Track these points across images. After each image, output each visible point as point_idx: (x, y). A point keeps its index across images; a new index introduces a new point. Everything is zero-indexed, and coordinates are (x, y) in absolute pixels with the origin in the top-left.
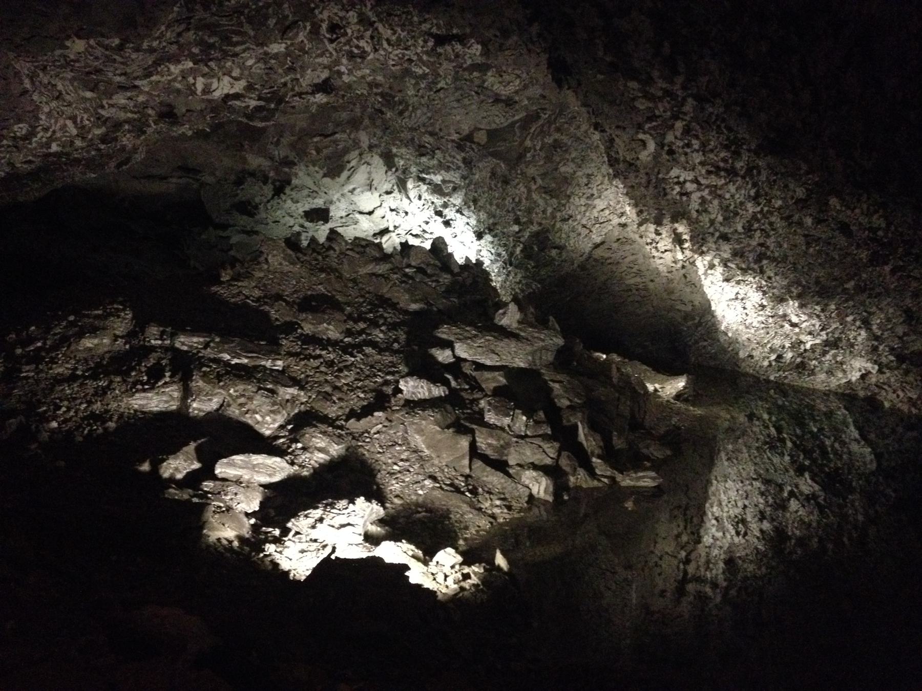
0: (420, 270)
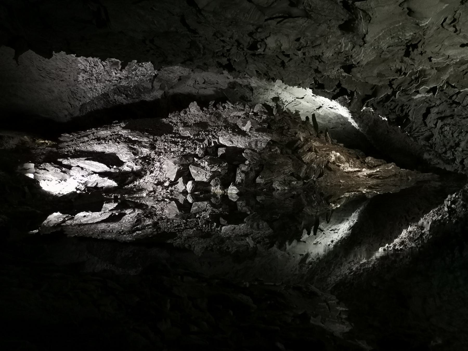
0: (256, 114)
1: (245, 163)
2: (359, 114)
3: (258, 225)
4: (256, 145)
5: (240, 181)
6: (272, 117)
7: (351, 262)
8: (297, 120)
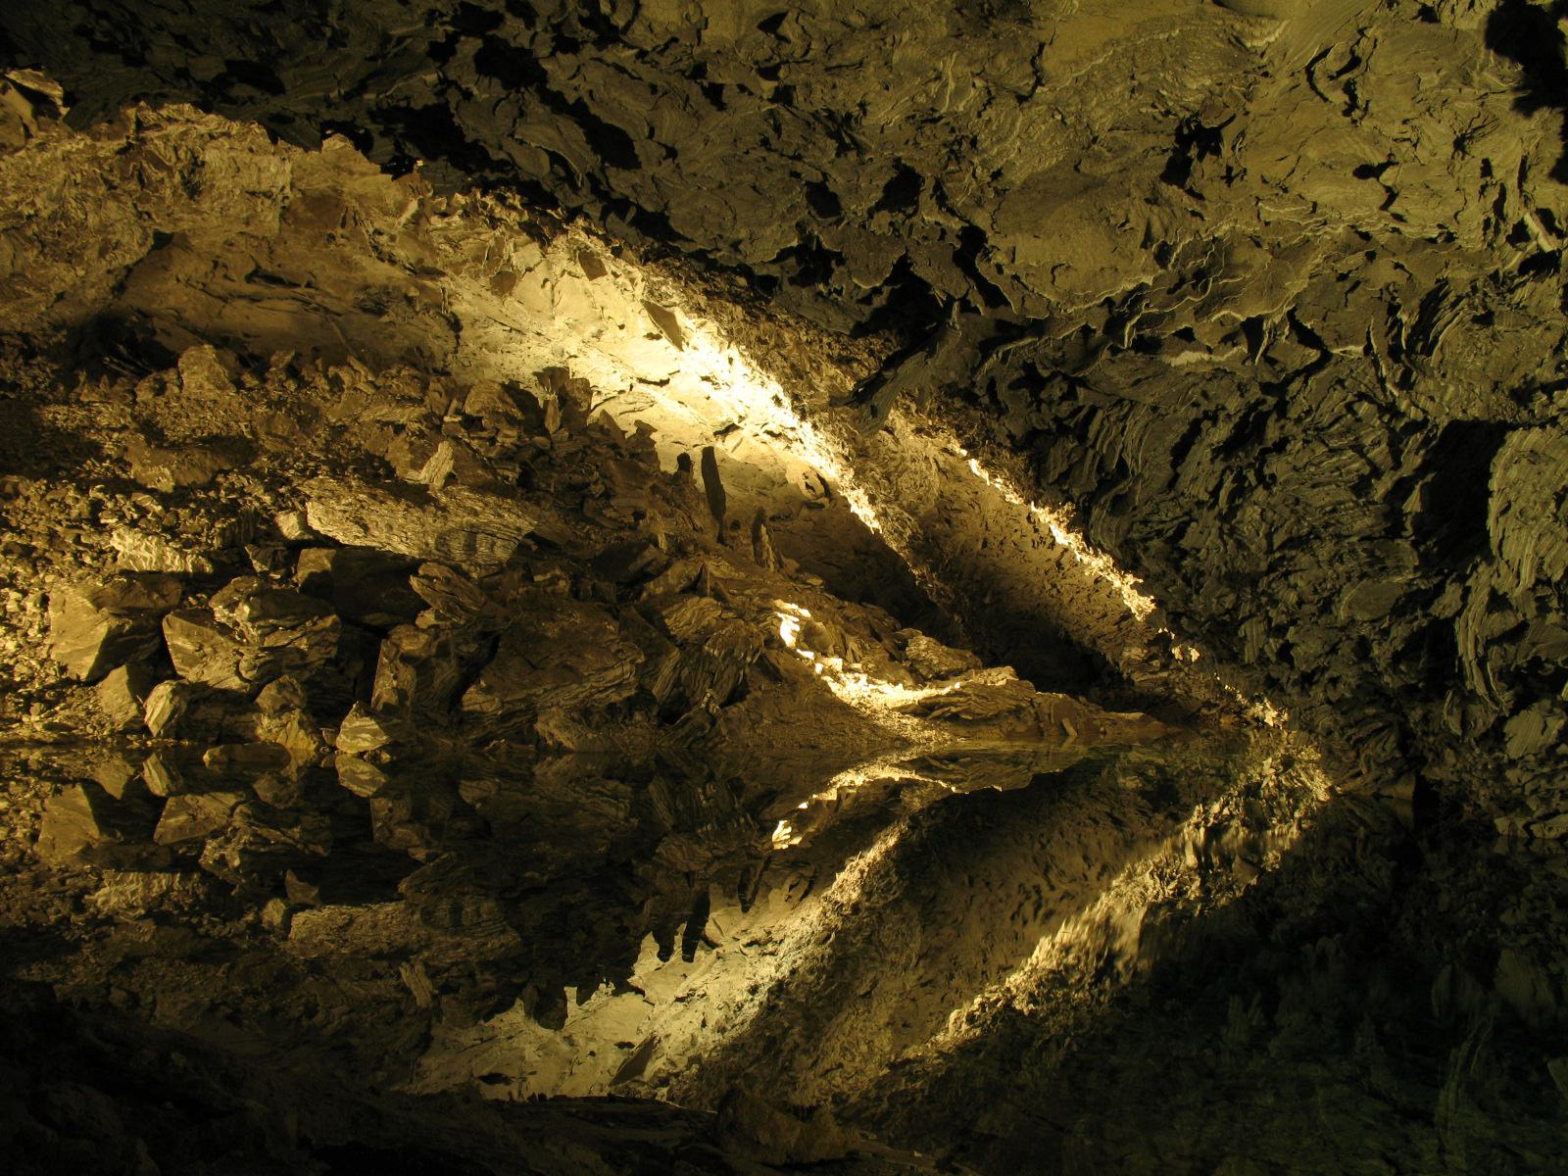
0: (471, 423)
1: (418, 622)
2: (883, 467)
3: (456, 911)
4: (470, 548)
5: (393, 699)
6: (539, 439)
7: (832, 1069)
8: (641, 465)
